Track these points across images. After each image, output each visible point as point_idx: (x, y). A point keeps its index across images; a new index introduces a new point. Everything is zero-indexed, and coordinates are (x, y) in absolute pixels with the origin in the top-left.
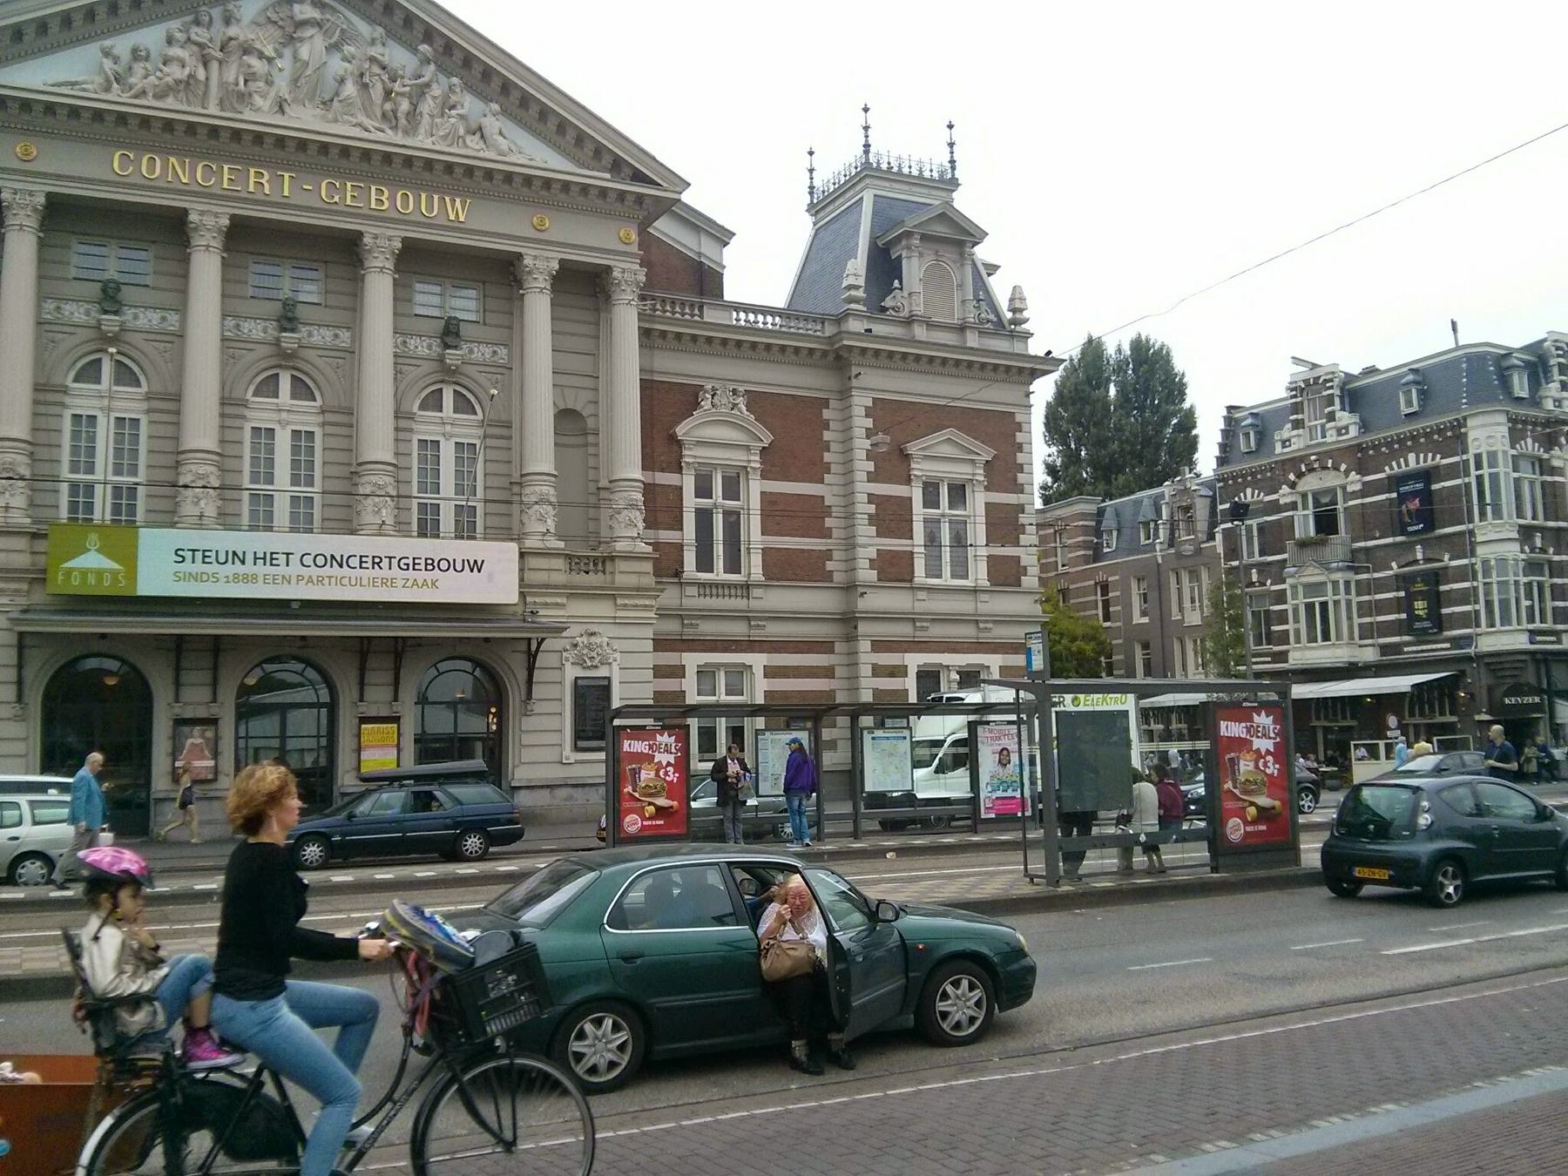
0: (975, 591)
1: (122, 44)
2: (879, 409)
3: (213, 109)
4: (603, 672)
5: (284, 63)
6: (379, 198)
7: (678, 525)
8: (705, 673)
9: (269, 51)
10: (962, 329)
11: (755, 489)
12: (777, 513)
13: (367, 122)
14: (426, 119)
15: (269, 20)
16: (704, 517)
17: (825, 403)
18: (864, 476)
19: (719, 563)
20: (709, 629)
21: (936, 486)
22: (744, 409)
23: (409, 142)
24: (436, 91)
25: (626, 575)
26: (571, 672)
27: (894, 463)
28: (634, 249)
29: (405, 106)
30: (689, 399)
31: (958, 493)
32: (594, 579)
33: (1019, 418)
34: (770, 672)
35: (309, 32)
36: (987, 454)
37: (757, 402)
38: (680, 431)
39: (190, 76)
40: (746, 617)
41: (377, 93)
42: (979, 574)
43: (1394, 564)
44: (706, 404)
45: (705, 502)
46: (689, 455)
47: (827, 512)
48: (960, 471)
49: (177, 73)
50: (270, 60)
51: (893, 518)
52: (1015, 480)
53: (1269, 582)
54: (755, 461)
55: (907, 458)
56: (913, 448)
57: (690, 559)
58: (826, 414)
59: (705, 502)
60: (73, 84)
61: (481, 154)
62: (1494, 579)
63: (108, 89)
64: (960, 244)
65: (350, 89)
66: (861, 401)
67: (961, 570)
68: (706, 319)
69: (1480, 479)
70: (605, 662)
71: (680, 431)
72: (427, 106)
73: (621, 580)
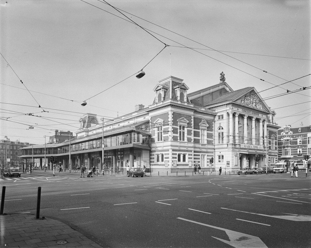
69: (309, 140)
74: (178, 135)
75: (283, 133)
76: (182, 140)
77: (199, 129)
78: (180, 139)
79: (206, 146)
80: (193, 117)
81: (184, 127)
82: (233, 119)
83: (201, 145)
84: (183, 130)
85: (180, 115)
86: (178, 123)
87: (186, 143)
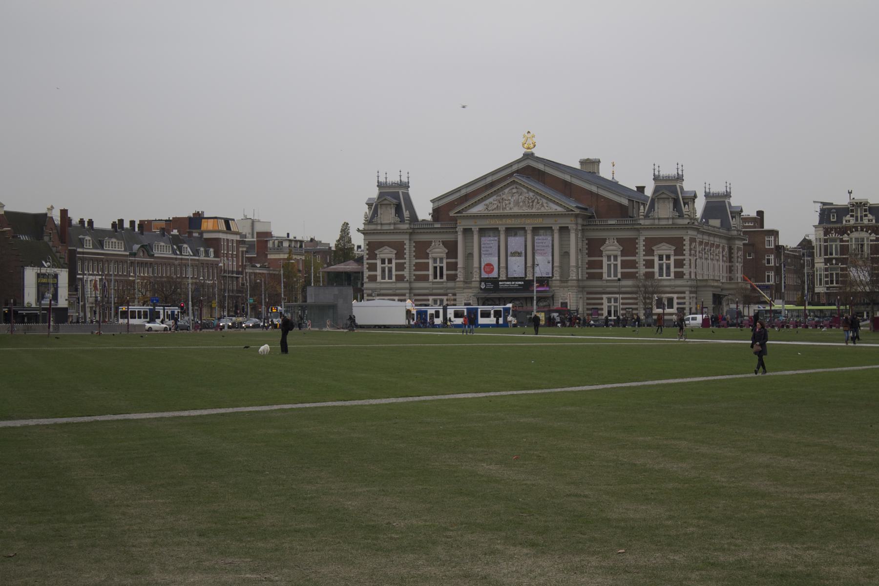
0: (670, 280)
1: (487, 202)
2: (646, 240)
3: (501, 211)
4: (566, 301)
5: (512, 200)
6: (528, 221)
7: (601, 268)
8: (609, 300)
9: (510, 198)
10: (668, 219)
11: (619, 259)
12: (624, 264)
13: (524, 208)
14: (534, 206)
15: (510, 193)
16: (609, 266)
17: (637, 238)
18: (642, 255)
19: (612, 275)
20: (608, 290)
21: (662, 256)
22: (616, 242)
23: (532, 211)
24: (536, 201)
25: (570, 284)
26: (561, 301)
27: (649, 251)
28: (573, 222)
29: (531, 204)
30: (603, 241)
31: (668, 257)
32: (565, 284)
33: (684, 238)
34: (623, 299)
35: (515, 194)
36: (674, 248)
37: (620, 241)
38: (601, 249)
39: (498, 206)
40: (620, 287)
41: (527, 203)
42: (672, 275)
43: (828, 264)
44: (607, 242)
45: (609, 263)
46: (604, 254)
47: (637, 263)
48: (668, 252)
49: (495, 206)
50: (510, 200)
51: (650, 264)
52: (683, 252)
53: (840, 264)
54: (619, 253)
55: (653, 251)
56: (654, 248)
57: (605, 276)
58: (637, 241)
59: (609, 263)
60: (480, 211)
61: (543, 211)
62: (818, 273)
63: (485, 210)
64: (669, 198)
65: (521, 204)
66: (642, 238)
67: (668, 274)
68: (609, 223)
70: (566, 299)
71: (601, 249)
72: (535, 204)
73: (569, 284)
74: (379, 272)
75: (848, 217)
76: (387, 278)
77: (428, 259)
78: (383, 277)
79: (444, 283)
80: (407, 242)
81: (390, 261)
82: (479, 235)
83: (431, 283)
84: (389, 263)
85: (381, 245)
86: (378, 256)
87: (394, 284)
